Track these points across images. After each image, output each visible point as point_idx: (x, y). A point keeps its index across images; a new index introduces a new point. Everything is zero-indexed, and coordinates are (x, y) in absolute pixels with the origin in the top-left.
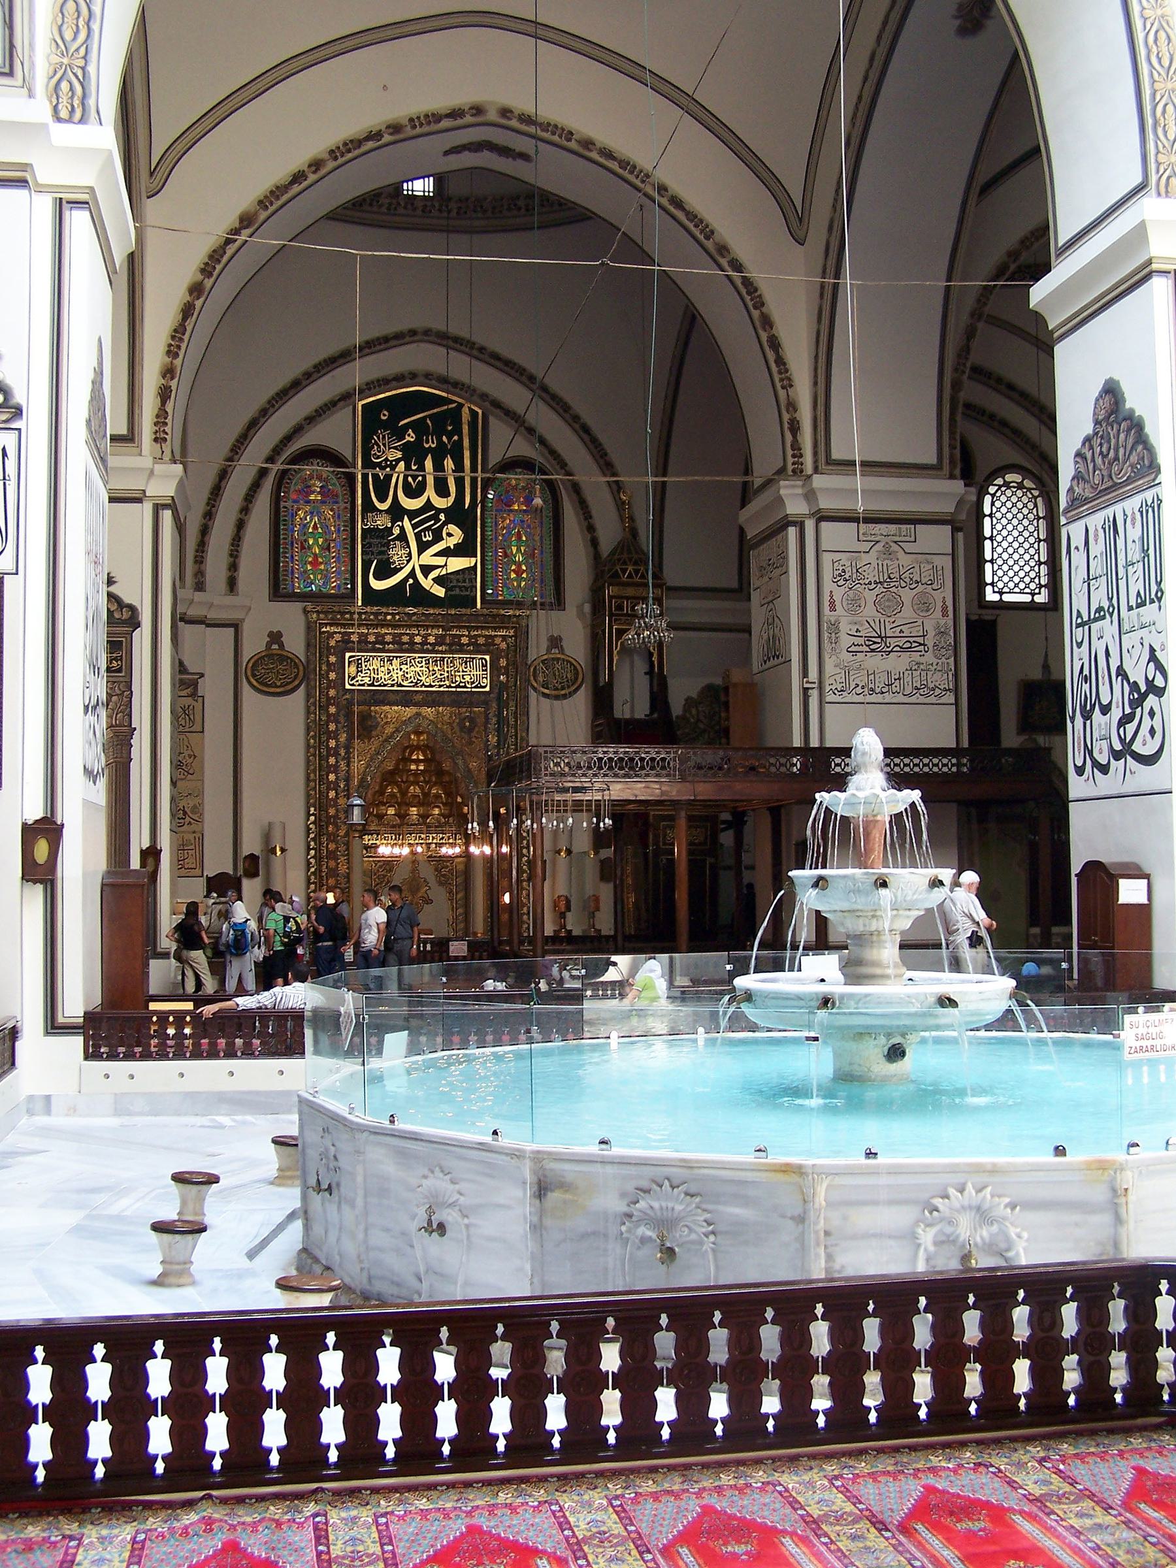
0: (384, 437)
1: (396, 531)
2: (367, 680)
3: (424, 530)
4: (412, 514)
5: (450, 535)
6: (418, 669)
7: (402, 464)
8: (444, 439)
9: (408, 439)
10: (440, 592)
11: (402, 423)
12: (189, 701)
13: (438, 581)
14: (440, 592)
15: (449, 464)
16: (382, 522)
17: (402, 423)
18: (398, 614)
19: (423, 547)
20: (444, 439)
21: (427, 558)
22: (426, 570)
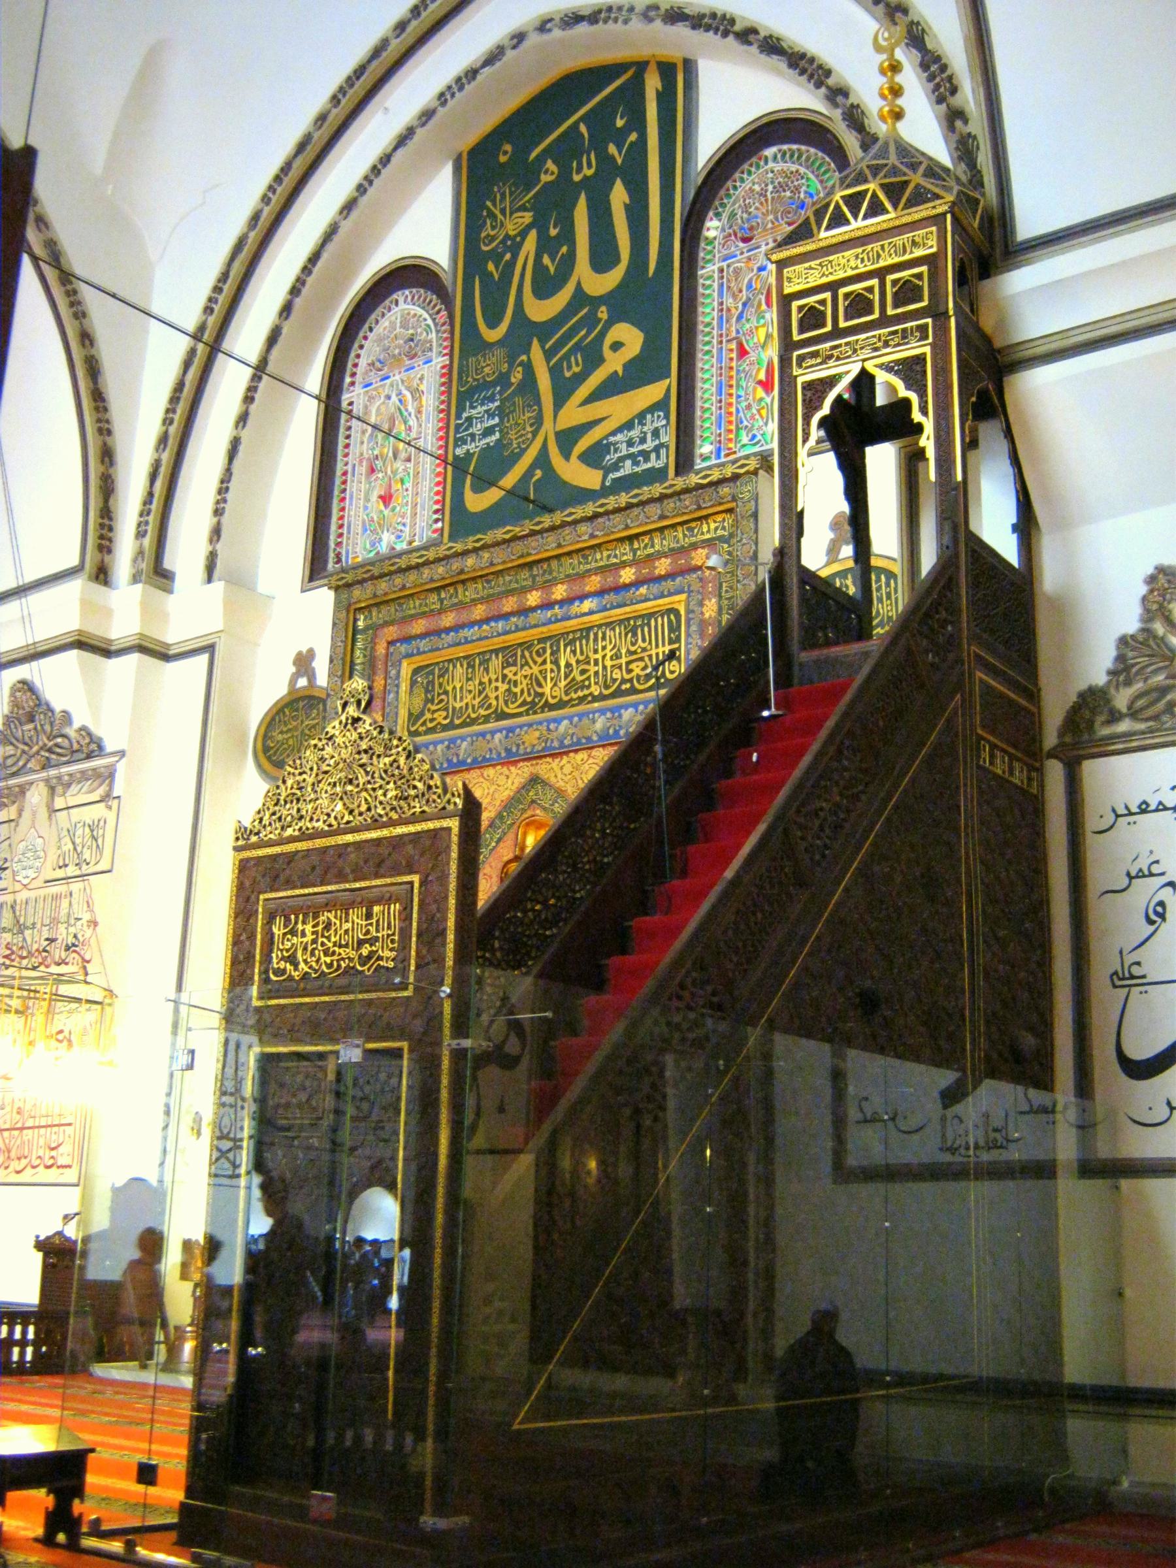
0: (503, 196)
1: (517, 376)
2: (440, 717)
3: (566, 357)
4: (544, 330)
5: (617, 346)
6: (536, 670)
7: (533, 234)
8: (612, 149)
9: (545, 178)
10: (590, 478)
11: (534, 155)
12: (99, 810)
13: (593, 457)
14: (590, 478)
15: (619, 195)
16: (489, 366)
17: (534, 155)
18: (485, 547)
19: (561, 396)
20: (612, 149)
21: (573, 414)
22: (567, 439)
